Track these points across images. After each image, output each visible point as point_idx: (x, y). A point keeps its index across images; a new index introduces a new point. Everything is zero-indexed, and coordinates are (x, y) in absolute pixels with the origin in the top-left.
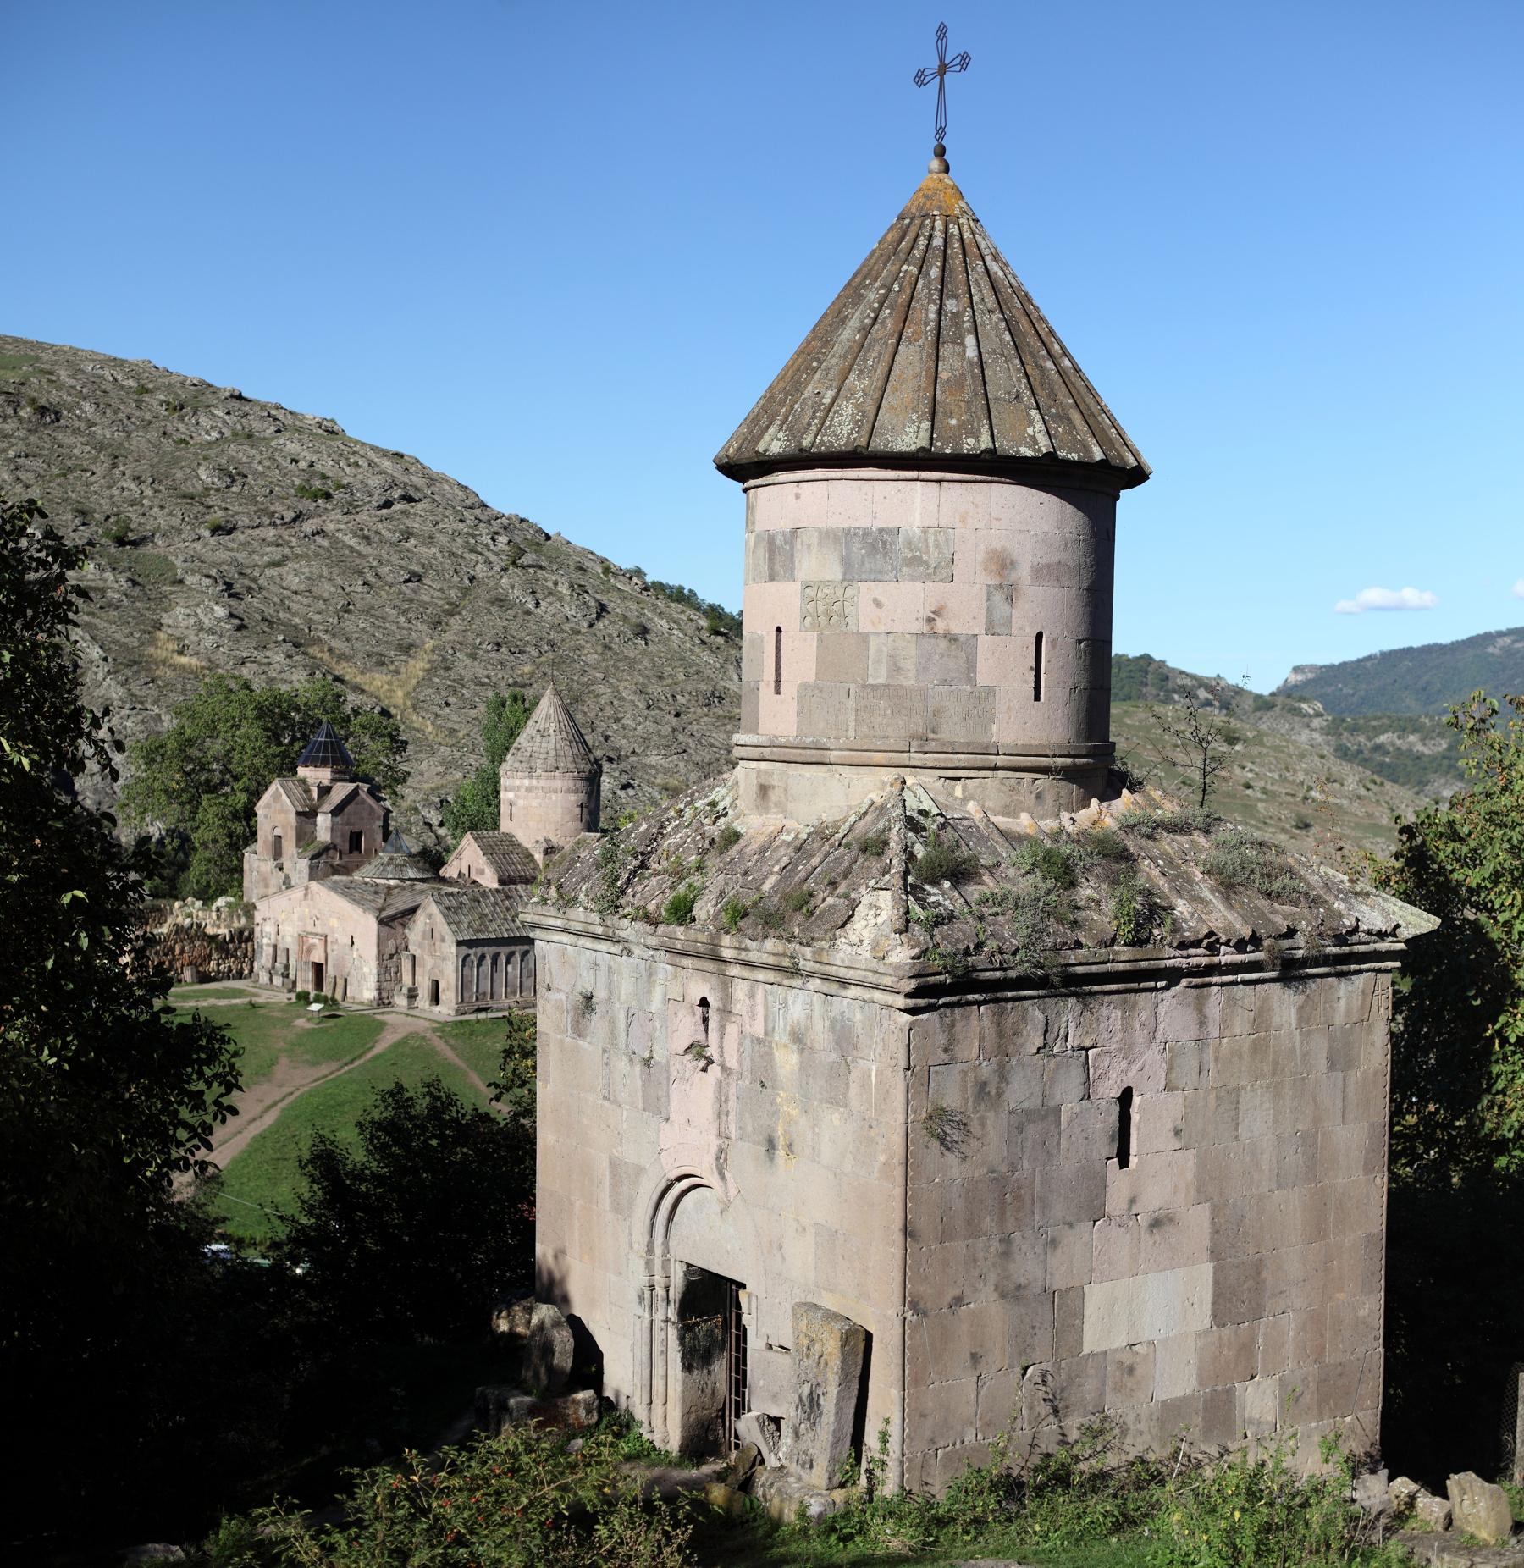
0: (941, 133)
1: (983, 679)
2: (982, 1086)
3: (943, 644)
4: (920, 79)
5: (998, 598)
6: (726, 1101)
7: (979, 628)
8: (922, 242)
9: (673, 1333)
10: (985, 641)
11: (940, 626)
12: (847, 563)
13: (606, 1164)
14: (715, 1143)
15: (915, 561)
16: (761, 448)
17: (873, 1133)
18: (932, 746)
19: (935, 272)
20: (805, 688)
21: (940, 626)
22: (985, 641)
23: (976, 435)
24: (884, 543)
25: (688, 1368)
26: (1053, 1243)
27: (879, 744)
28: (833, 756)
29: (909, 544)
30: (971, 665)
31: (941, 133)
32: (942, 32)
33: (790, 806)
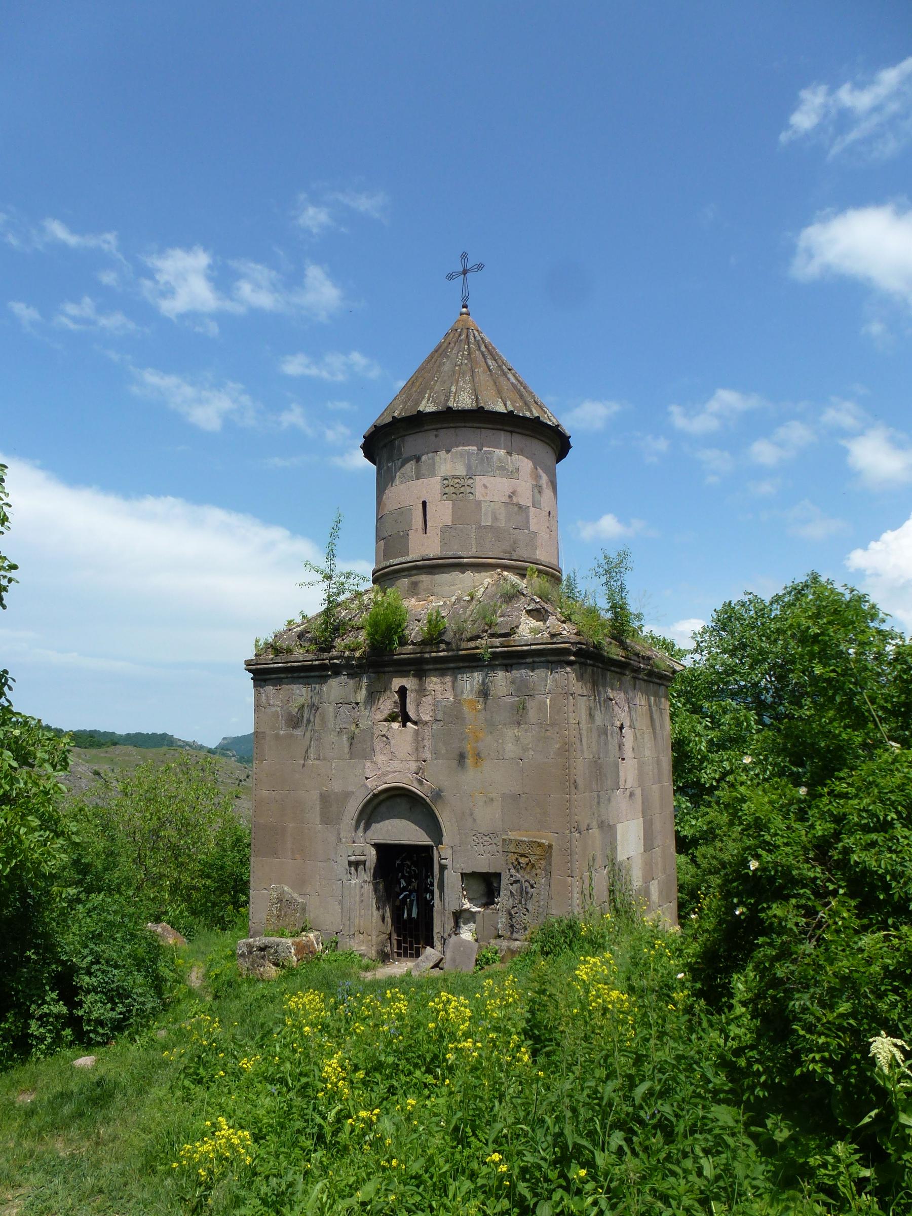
0: (465, 298)
1: (533, 528)
2: (591, 709)
3: (516, 509)
4: (450, 277)
5: (536, 491)
6: (423, 739)
7: (530, 504)
8: (472, 338)
9: (368, 888)
10: (532, 509)
11: (515, 500)
12: (469, 467)
13: (315, 795)
14: (413, 766)
15: (502, 468)
16: (421, 408)
17: (548, 733)
18: (514, 557)
19: (483, 348)
20: (445, 530)
21: (515, 500)
22: (532, 509)
23: (531, 411)
24: (487, 458)
25: (378, 909)
26: (609, 800)
27: (490, 554)
28: (465, 560)
29: (499, 460)
30: (528, 522)
31: (465, 298)
32: (464, 256)
33: (436, 590)
